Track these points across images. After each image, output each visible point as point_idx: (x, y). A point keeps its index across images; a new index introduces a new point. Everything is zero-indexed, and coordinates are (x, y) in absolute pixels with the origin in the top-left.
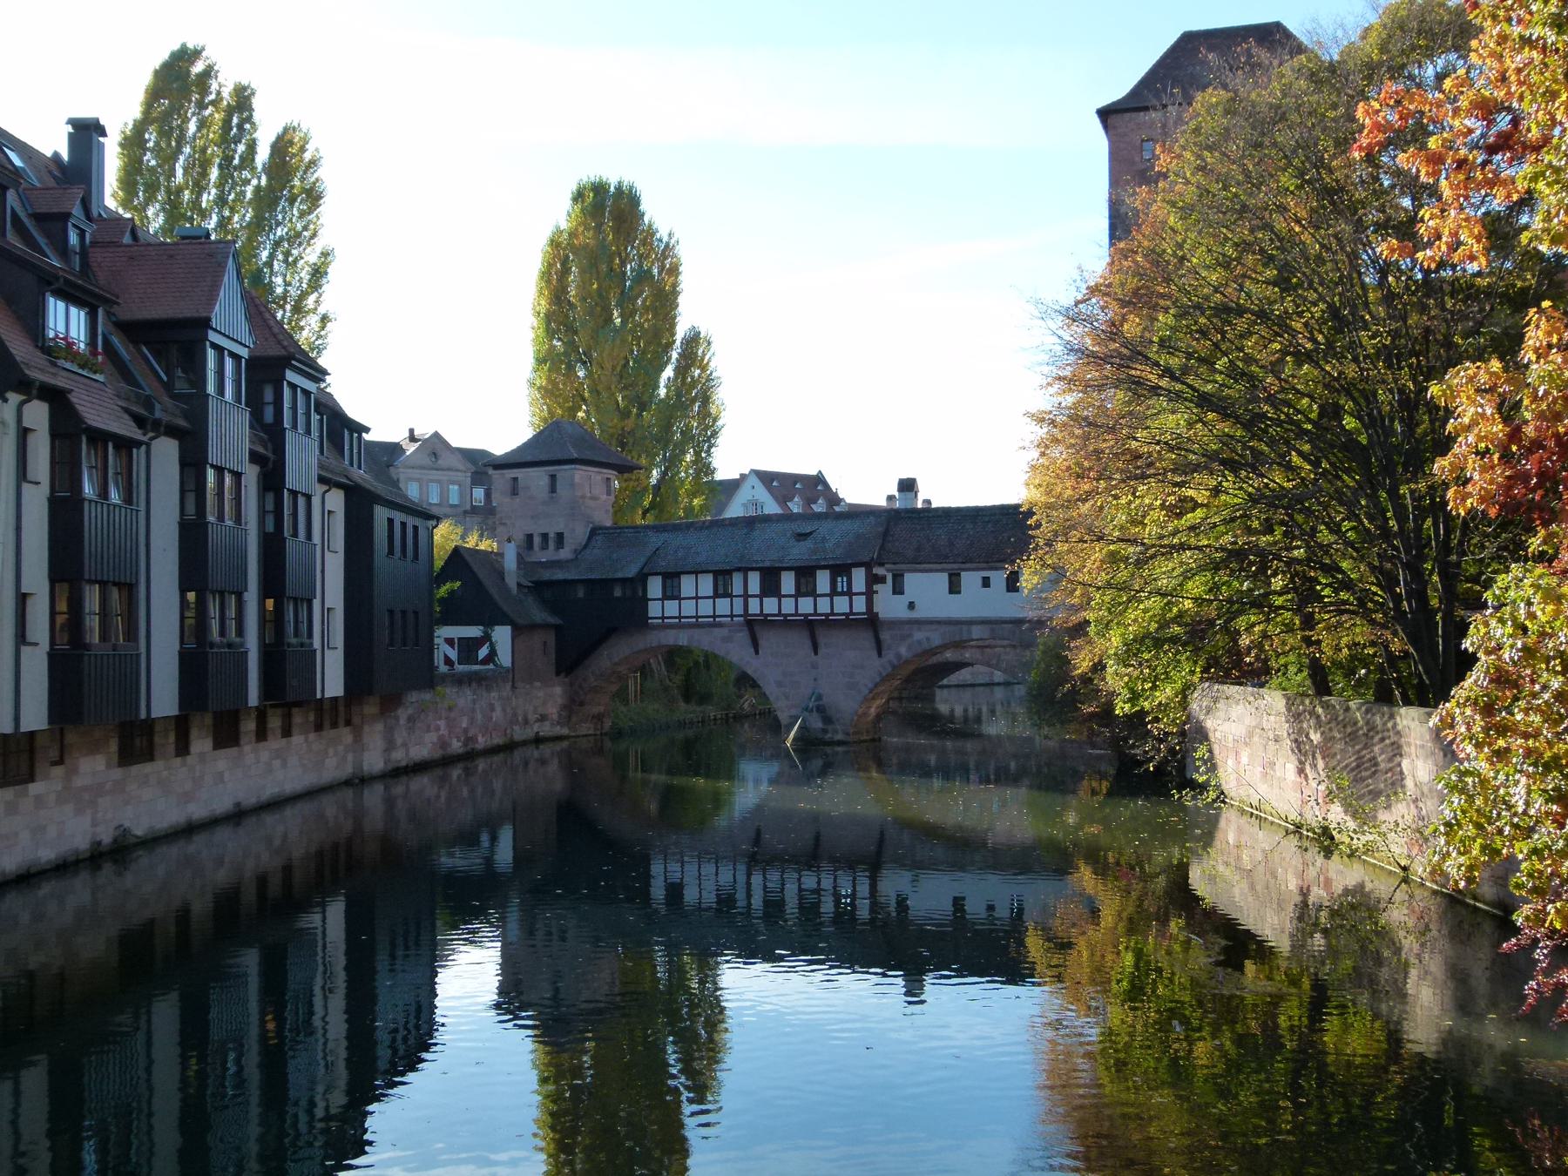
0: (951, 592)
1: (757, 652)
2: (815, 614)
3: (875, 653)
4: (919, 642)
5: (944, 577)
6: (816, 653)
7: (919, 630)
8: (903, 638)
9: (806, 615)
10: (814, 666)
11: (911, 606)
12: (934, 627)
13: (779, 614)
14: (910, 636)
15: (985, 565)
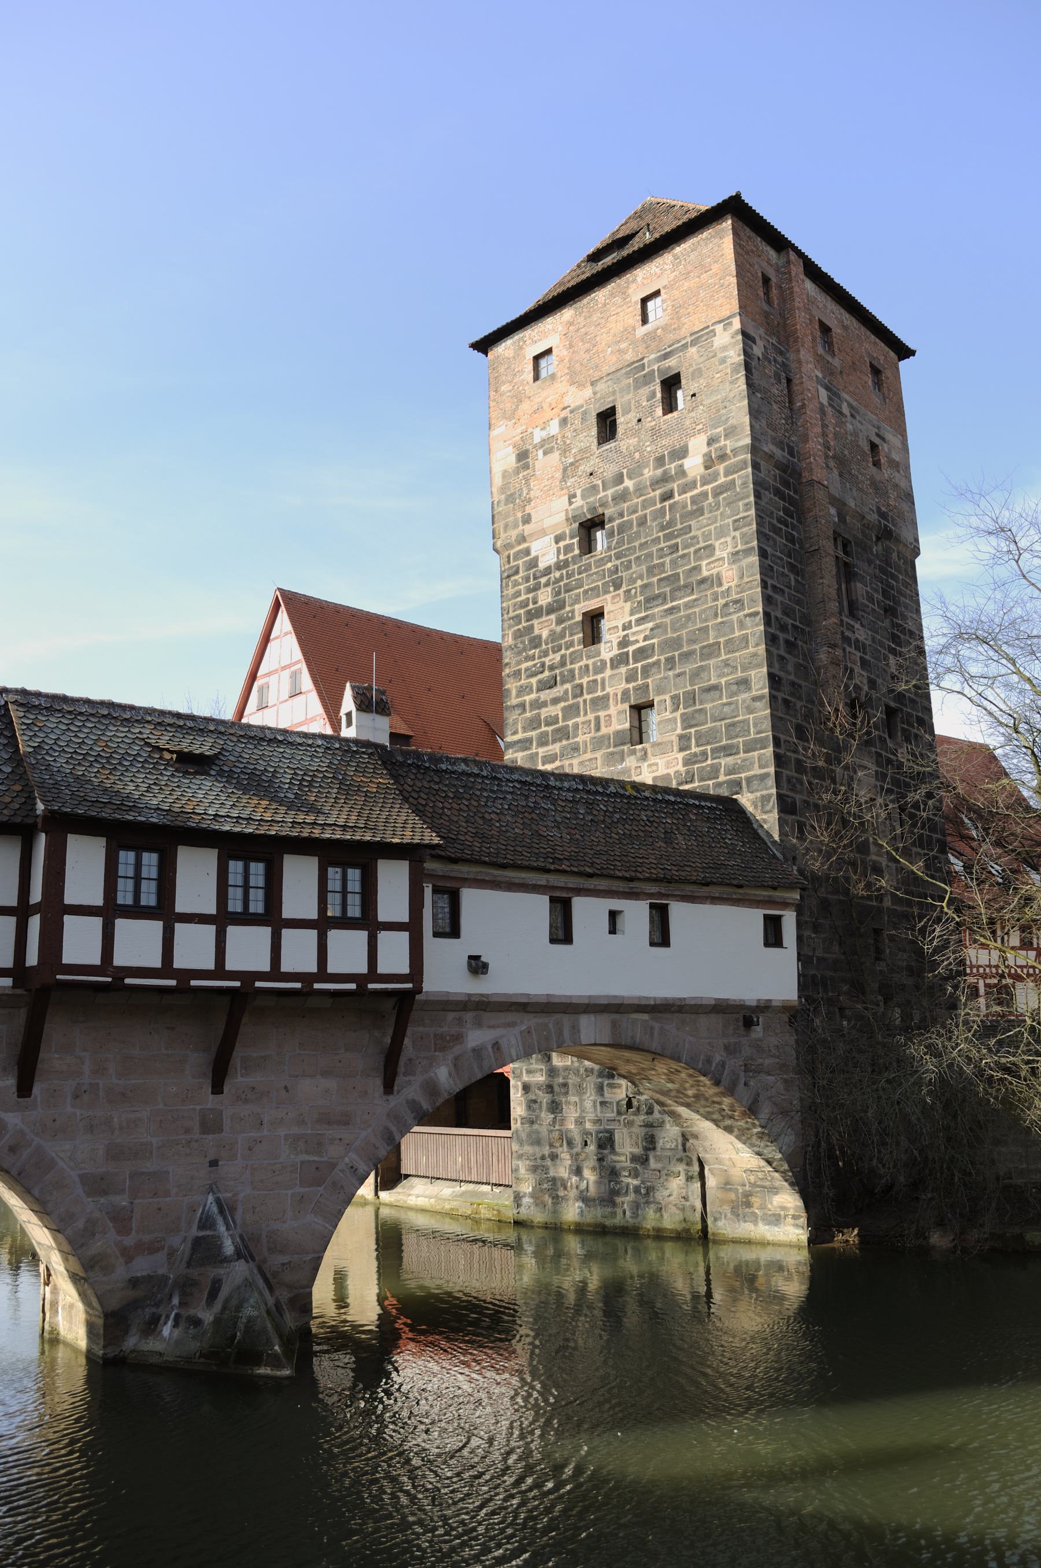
0: (611, 932)
1: (24, 1089)
2: (275, 972)
3: (378, 1082)
4: (477, 1052)
5: (541, 904)
6: (217, 1088)
7: (478, 1024)
8: (445, 1043)
9: (248, 977)
10: (211, 1124)
11: (477, 966)
12: (511, 1017)
13: (167, 968)
14: (458, 1038)
15: (621, 886)
